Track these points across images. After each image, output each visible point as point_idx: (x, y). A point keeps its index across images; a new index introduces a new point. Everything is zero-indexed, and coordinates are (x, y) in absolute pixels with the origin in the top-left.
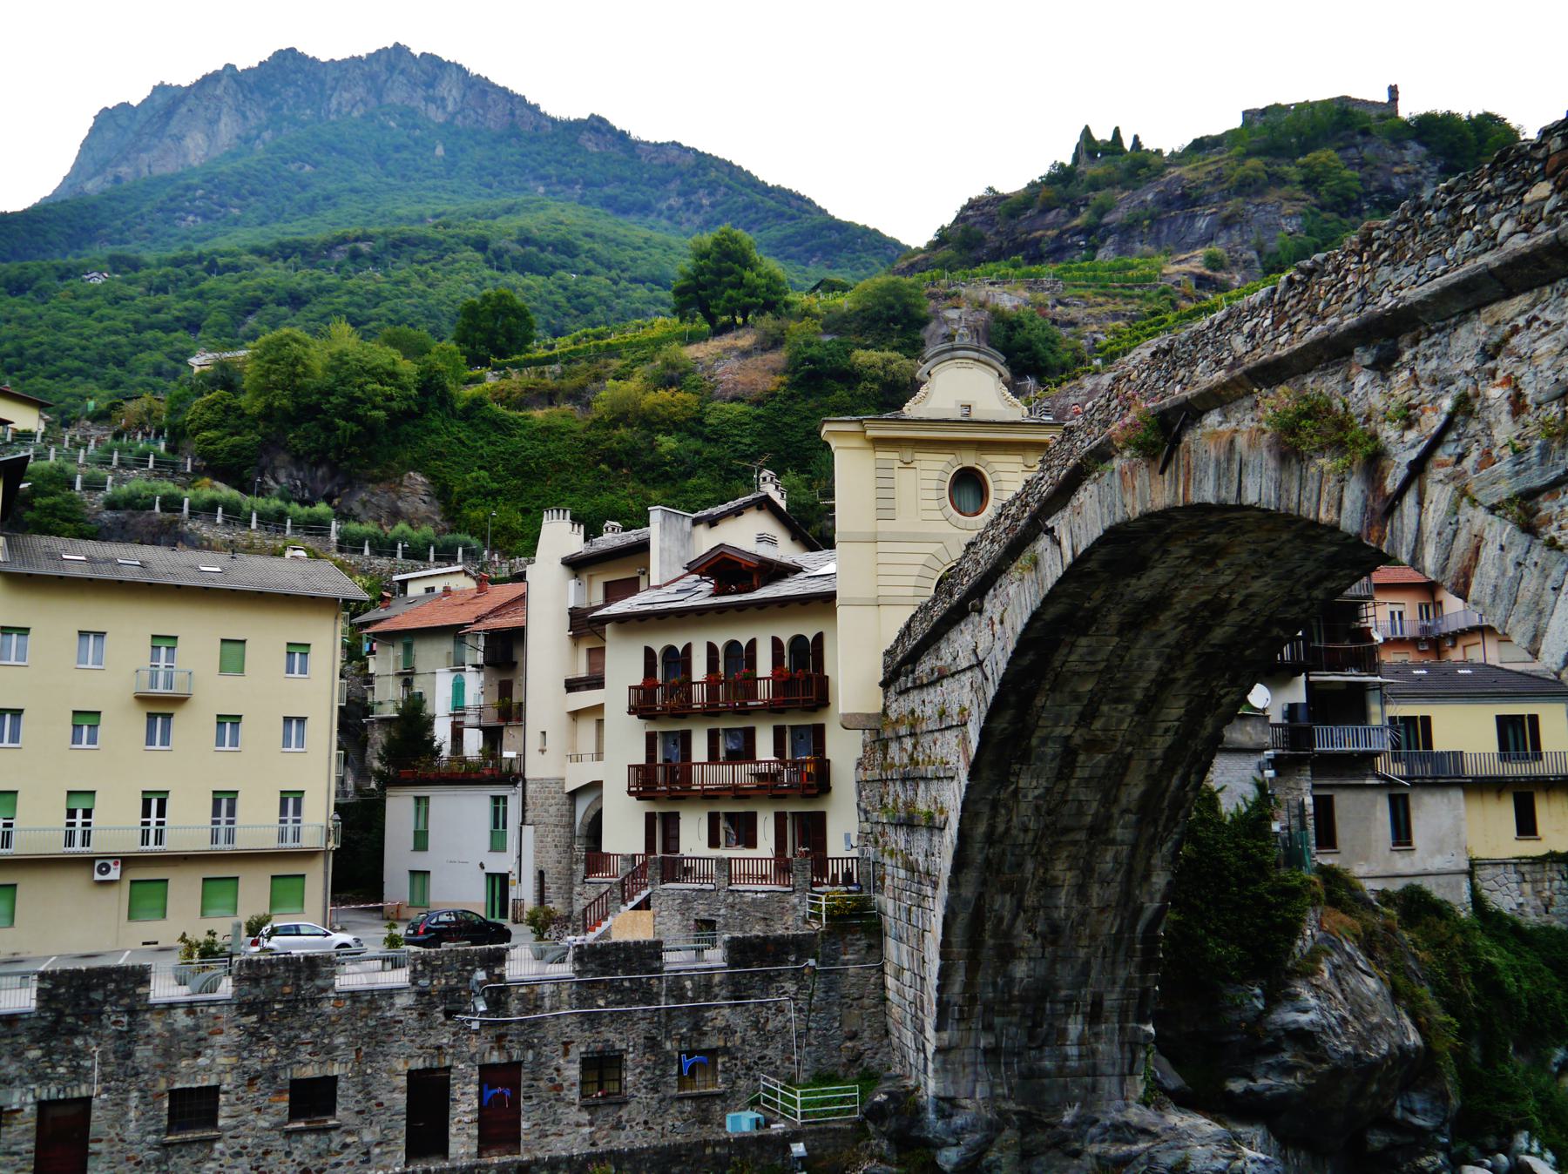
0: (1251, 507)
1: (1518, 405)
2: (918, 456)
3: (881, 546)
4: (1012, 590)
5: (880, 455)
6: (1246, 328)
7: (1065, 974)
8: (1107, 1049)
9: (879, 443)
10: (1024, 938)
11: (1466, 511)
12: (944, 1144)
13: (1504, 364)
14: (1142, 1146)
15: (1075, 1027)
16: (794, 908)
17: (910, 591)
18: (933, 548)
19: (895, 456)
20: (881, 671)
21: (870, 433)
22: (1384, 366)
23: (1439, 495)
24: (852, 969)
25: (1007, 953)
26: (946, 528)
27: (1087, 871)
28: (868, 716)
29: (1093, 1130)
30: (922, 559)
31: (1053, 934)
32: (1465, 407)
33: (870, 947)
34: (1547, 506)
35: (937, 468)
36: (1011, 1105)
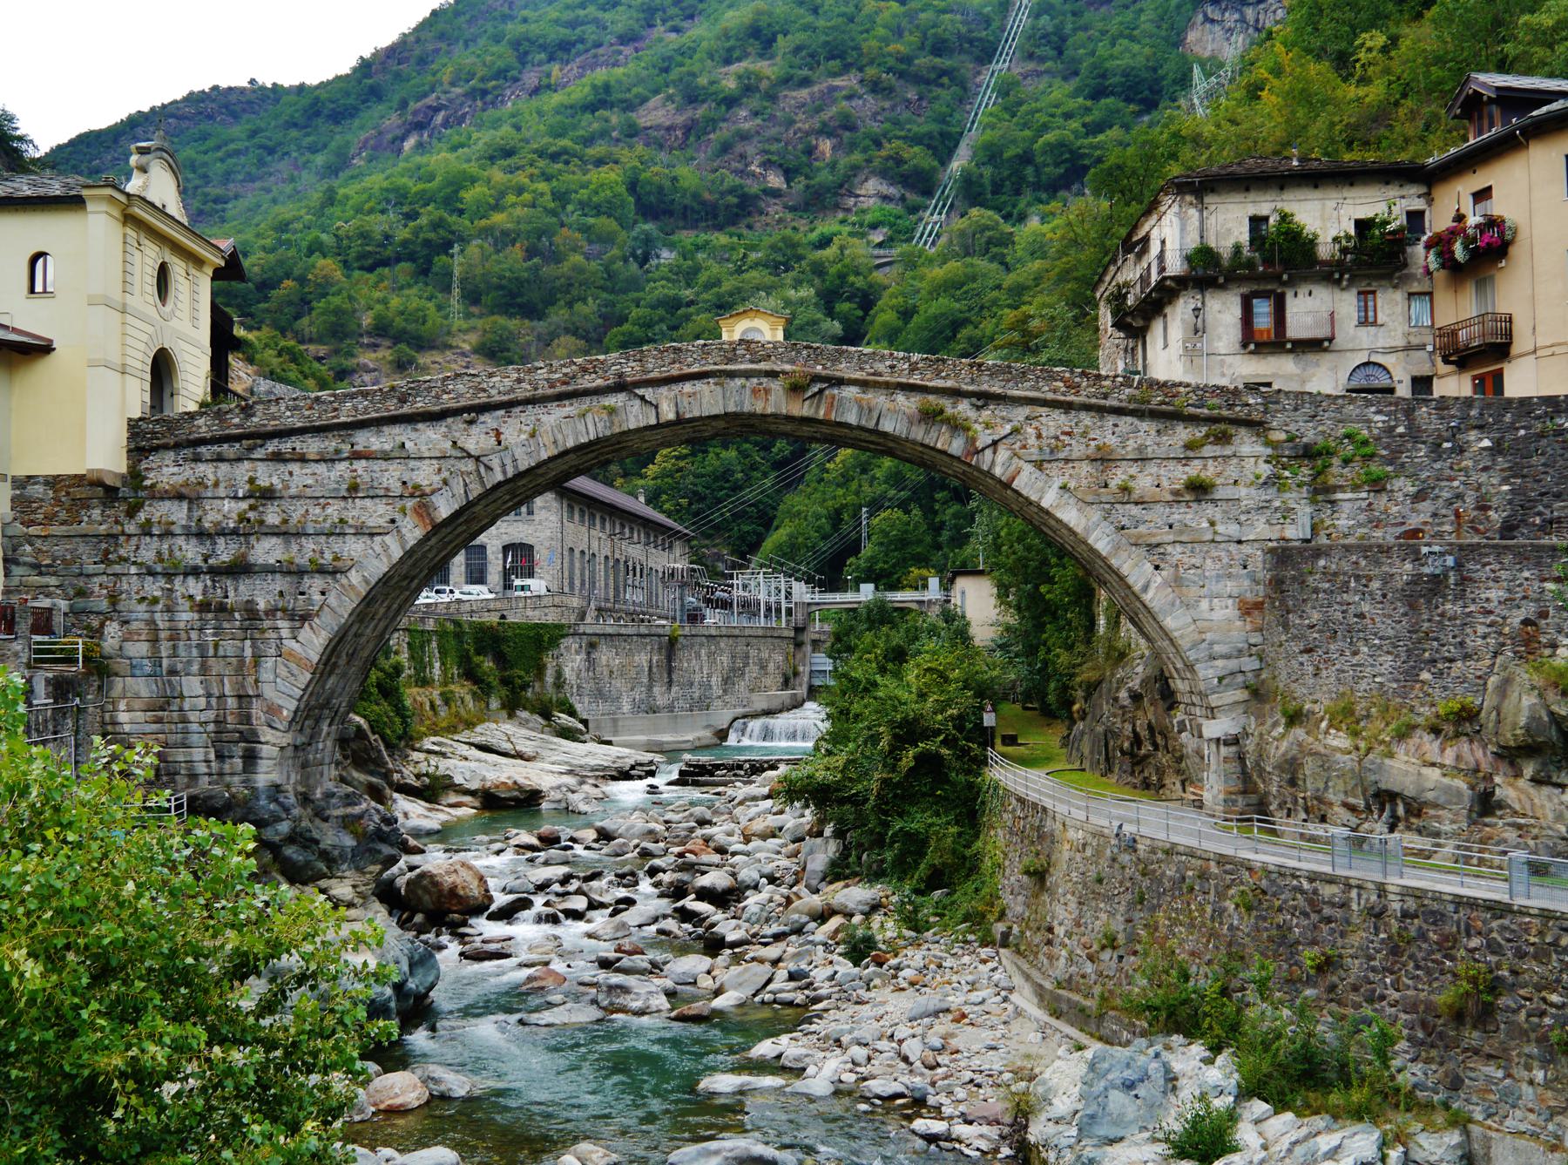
0: (885, 435)
1: (1039, 436)
2: (147, 242)
3: (129, 319)
4: (544, 418)
5: (129, 231)
6: (888, 363)
7: (341, 684)
8: (329, 743)
9: (129, 219)
10: (343, 661)
11: (1016, 460)
12: (278, 819)
13: (1035, 424)
14: (364, 806)
15: (325, 728)
16: (16, 655)
17: (139, 365)
18: (150, 329)
19: (134, 234)
20: (126, 435)
21: (137, 211)
22: (979, 408)
23: (1003, 454)
24: (91, 710)
25: (330, 675)
26: (151, 312)
27: (389, 608)
28: (116, 475)
29: (334, 801)
30: (145, 337)
31: (351, 657)
32: (1016, 431)
33: (100, 688)
34: (1046, 465)
35: (150, 256)
36: (300, 789)
